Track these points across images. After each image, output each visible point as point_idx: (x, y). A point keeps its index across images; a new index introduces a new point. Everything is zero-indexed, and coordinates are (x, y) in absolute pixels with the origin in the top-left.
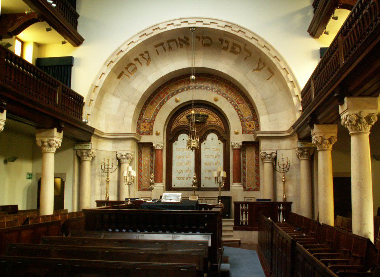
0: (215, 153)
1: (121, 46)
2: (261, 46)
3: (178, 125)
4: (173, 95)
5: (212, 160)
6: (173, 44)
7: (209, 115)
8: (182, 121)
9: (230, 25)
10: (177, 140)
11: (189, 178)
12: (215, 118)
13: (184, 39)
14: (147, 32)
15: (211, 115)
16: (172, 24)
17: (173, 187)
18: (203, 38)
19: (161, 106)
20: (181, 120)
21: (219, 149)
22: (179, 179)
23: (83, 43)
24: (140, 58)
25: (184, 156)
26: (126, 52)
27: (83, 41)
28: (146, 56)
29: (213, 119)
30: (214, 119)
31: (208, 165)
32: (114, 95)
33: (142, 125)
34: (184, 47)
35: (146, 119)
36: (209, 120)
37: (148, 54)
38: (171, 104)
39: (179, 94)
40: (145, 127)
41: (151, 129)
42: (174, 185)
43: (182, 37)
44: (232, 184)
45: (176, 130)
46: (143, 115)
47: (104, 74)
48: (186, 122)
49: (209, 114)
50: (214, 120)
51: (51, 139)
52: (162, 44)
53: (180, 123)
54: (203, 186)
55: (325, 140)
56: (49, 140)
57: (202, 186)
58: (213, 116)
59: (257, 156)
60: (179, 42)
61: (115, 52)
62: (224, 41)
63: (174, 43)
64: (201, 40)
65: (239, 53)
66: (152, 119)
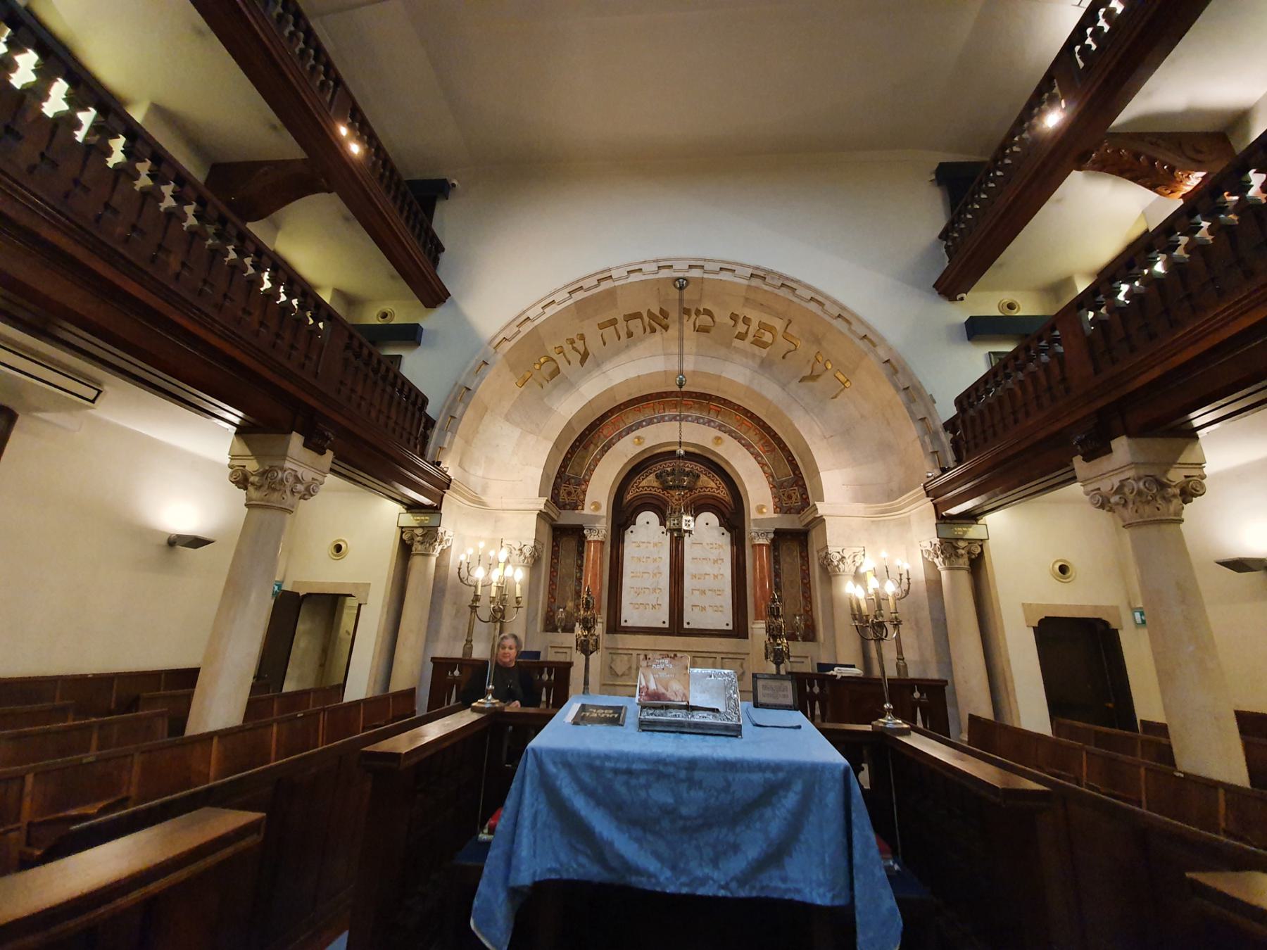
0: (714, 554)
1: (528, 309)
2: (831, 316)
3: (637, 492)
4: (630, 430)
5: (708, 568)
6: (636, 325)
9: (762, 274)
10: (635, 524)
11: (657, 607)
12: (713, 480)
13: (659, 315)
14: (586, 284)
15: (705, 474)
17: (623, 624)
18: (698, 312)
19: (604, 451)
20: (644, 483)
21: (721, 546)
22: (637, 606)
23: (447, 301)
24: (568, 347)
26: (537, 322)
27: (447, 298)
28: (579, 345)
29: (710, 484)
30: (712, 482)
32: (507, 418)
35: (573, 478)
36: (700, 484)
38: (625, 451)
39: (642, 430)
40: (569, 494)
42: (664, 622)
43: (656, 311)
44: (753, 623)
45: (632, 503)
47: (486, 364)
48: (653, 487)
49: (701, 472)
50: (712, 484)
51: (276, 463)
52: (613, 322)
53: (641, 489)
54: (688, 623)
55: (1170, 486)
56: (270, 467)
57: (686, 626)
58: (709, 477)
60: (649, 322)
61: (514, 320)
62: (741, 320)
64: (693, 316)
65: (771, 344)
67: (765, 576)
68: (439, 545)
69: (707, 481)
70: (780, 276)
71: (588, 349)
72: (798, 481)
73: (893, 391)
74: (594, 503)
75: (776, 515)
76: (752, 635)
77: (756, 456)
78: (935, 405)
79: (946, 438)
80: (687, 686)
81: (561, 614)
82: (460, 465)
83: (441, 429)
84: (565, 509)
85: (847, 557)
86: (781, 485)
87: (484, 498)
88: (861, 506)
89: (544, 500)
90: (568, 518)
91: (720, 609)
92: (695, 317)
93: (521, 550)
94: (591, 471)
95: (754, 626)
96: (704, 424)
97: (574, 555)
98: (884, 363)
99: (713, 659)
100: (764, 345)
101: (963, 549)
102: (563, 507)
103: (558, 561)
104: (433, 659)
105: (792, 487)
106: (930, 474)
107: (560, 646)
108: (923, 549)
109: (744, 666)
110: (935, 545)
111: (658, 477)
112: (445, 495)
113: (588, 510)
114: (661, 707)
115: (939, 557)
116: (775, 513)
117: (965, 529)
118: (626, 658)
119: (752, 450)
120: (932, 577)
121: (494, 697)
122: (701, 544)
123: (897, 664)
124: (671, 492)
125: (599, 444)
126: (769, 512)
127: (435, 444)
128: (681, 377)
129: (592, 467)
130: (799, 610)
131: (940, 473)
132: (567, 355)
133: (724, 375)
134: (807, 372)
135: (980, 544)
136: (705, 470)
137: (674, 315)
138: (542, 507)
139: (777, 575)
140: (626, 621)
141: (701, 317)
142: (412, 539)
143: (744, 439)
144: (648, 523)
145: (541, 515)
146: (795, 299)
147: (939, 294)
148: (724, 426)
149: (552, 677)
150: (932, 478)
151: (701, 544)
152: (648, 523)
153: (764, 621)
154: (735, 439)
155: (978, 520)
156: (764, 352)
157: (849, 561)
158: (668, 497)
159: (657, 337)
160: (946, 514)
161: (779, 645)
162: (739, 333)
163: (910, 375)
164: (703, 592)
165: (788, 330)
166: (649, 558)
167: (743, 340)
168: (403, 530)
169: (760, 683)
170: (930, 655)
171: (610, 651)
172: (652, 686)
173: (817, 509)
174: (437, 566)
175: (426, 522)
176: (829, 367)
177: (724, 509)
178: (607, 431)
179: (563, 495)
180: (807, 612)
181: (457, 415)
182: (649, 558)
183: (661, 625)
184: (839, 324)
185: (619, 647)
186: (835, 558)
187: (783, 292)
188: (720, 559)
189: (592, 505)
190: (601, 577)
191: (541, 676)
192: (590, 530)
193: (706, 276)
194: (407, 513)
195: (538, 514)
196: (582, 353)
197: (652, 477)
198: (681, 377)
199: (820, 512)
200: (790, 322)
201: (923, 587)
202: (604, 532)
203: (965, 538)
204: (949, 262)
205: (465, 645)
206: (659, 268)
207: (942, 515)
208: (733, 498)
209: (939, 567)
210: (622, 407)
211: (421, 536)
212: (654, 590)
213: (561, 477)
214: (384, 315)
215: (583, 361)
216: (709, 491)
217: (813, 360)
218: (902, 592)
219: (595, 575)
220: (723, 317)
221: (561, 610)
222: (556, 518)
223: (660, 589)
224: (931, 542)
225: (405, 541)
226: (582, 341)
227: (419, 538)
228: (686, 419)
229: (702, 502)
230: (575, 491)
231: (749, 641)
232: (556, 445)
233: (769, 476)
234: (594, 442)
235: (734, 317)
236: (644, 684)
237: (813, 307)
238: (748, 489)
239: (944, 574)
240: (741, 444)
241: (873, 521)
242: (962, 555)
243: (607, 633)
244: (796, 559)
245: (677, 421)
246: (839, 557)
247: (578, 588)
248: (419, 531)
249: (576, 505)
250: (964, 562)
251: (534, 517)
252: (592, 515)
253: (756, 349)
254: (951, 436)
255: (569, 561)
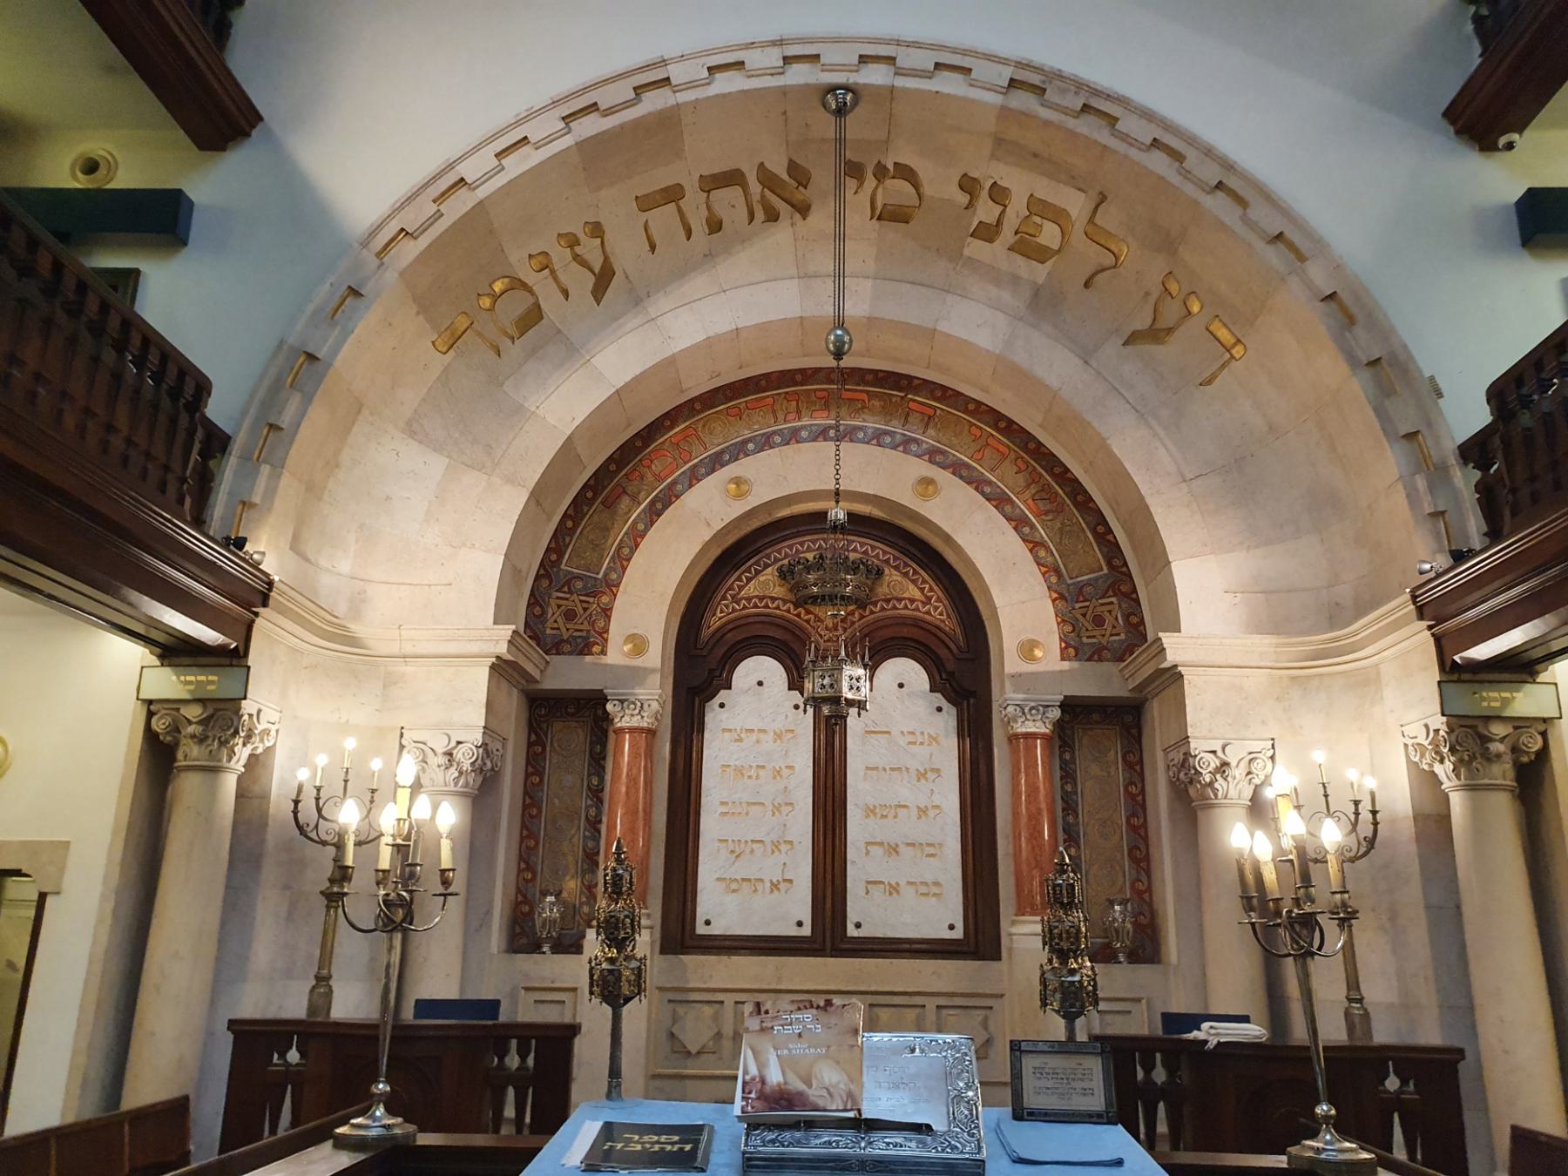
2: (1200, 184)
3: (734, 610)
4: (716, 463)
5: (905, 792)
6: (729, 202)
7: (887, 571)
8: (757, 593)
9: (1035, 79)
10: (730, 688)
11: (783, 886)
12: (914, 582)
13: (785, 177)
14: (605, 98)
15: (896, 568)
16: (739, 65)
17: (701, 929)
18: (881, 172)
19: (654, 513)
22: (734, 886)
23: (254, 133)
24: (560, 255)
25: (763, 767)
26: (482, 192)
28: (590, 249)
30: (911, 586)
31: (883, 816)
32: (412, 430)
33: (553, 602)
34: (784, 222)
35: (579, 577)
36: (883, 590)
37: (602, 243)
40: (570, 615)
41: (601, 624)
43: (780, 169)
44: (1014, 923)
46: (561, 557)
48: (773, 599)
50: (917, 594)
52: (673, 194)
54: (858, 925)
57: (852, 931)
58: (906, 575)
59: (1136, 779)
60: (763, 196)
61: (426, 185)
62: (984, 194)
63: (735, 193)
64: (870, 183)
66: (606, 574)
67: (1039, 812)
68: (244, 745)
69: (900, 583)
70: (1079, 85)
71: (612, 259)
72: (1120, 582)
73: (1344, 368)
74: (632, 638)
75: (1066, 665)
76: (1010, 950)
77: (1019, 523)
78: (1441, 401)
79: (1465, 480)
80: (856, 1076)
81: (549, 909)
82: (296, 545)
83: (245, 458)
84: (558, 653)
85: (1234, 764)
86: (1079, 593)
87: (357, 629)
88: (1264, 645)
89: (506, 631)
90: (567, 674)
91: (935, 890)
92: (874, 183)
93: (449, 754)
94: (622, 561)
95: (1014, 930)
96: (894, 448)
97: (582, 763)
98: (1323, 300)
99: (918, 1010)
100: (1039, 254)
101: (1502, 740)
102: (555, 647)
103: (541, 781)
104: (233, 1024)
105: (1103, 597)
106: (1427, 567)
107: (545, 985)
108: (1410, 742)
109: (991, 1023)
110: (1437, 731)
111: (783, 574)
112: (259, 621)
113: (616, 653)
114: (795, 1125)
115: (1446, 760)
116: (1063, 659)
117: (1507, 695)
118: (708, 1010)
119: (1008, 508)
120: (1429, 808)
121: (390, 1111)
122: (888, 733)
123: (1347, 1014)
124: (816, 610)
125: (642, 494)
126: (1050, 658)
127: (230, 494)
128: (839, 332)
129: (626, 551)
130: (1121, 890)
131: (1450, 562)
132: (559, 274)
133: (943, 327)
134: (1142, 321)
135: (1541, 728)
136: (896, 559)
137: (823, 176)
138: (502, 649)
139: (1070, 806)
140: (708, 923)
141: (889, 182)
142: (175, 729)
143: (990, 483)
144: (760, 684)
145: (502, 670)
146: (1113, 143)
147: (1458, 133)
148: (943, 452)
149: (530, 1061)
150: (1432, 574)
151: (888, 733)
152: (760, 684)
153: (1039, 918)
154: (969, 483)
155: (1538, 673)
156: (1040, 272)
157: (1238, 772)
158: (808, 621)
159: (781, 234)
160: (1461, 658)
161: (1072, 972)
162: (980, 222)
163: (1383, 331)
164: (893, 849)
165: (1098, 220)
166: (763, 767)
167: (991, 241)
168: (152, 707)
169: (1029, 1063)
170: (1427, 996)
171: (671, 996)
172: (775, 1076)
173: (1164, 649)
174: (241, 795)
175: (210, 687)
176: (1195, 308)
177: (943, 652)
178: (661, 466)
179: (554, 618)
180: (1140, 893)
181: (285, 420)
182: (763, 767)
183: (793, 931)
184: (1217, 204)
185: (691, 985)
186: (1207, 765)
187: (1086, 127)
188: (933, 770)
189: (626, 642)
190: (648, 813)
191: (501, 1059)
192: (622, 702)
193: (901, 82)
194: (162, 665)
195: (493, 667)
196: (597, 271)
197: (770, 575)
198: (839, 332)
199: (1172, 657)
200: (1103, 199)
201: (1407, 829)
202: (655, 705)
203: (1504, 715)
204: (1481, 56)
205: (314, 988)
206: (787, 60)
207: (1454, 660)
208: (962, 622)
209: (1446, 785)
210: (698, 406)
211: (199, 723)
212: (776, 845)
213: (548, 576)
214: (91, 167)
215: (599, 291)
216: (906, 607)
217: (1156, 292)
218: (1359, 843)
219: (631, 813)
220: (941, 185)
221: (550, 899)
222: (536, 674)
223: (791, 842)
224: (1426, 726)
225: (156, 735)
226: (599, 240)
227: (191, 729)
228: (848, 435)
229: (887, 633)
230: (585, 610)
231: (1002, 966)
232: (538, 496)
233: (1049, 570)
234: (629, 489)
235: (968, 185)
236: (753, 1071)
237: (1159, 163)
238: (998, 602)
239: (1457, 801)
240: (983, 494)
241: (1293, 678)
242: (1499, 756)
243: (662, 952)
244: (1112, 770)
245: (831, 439)
246: (1214, 763)
247: (590, 844)
248: (193, 712)
249: (587, 642)
250: (1503, 772)
251: (484, 673)
252: (627, 667)
253: (1022, 266)
254: (1477, 474)
255: (569, 780)
